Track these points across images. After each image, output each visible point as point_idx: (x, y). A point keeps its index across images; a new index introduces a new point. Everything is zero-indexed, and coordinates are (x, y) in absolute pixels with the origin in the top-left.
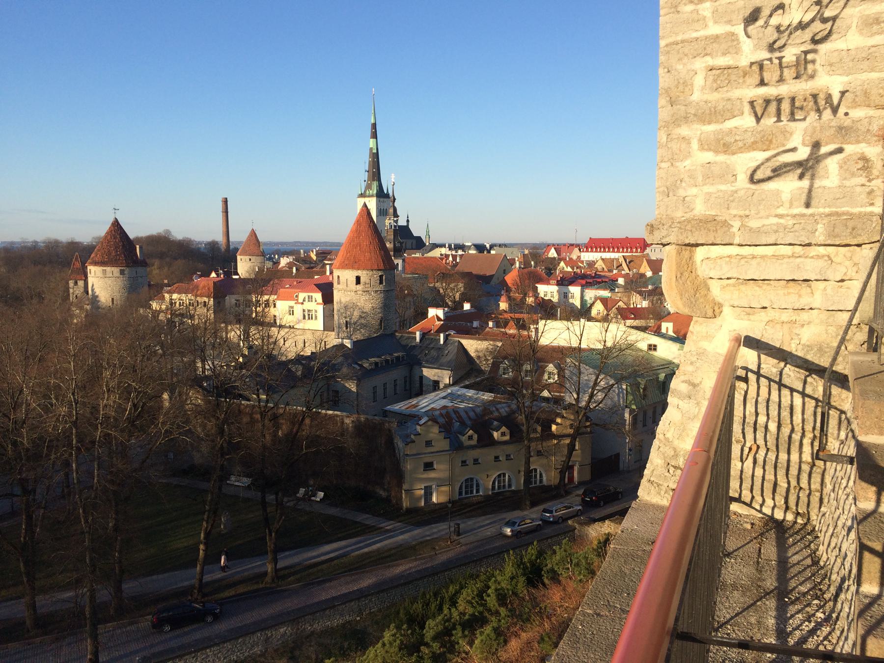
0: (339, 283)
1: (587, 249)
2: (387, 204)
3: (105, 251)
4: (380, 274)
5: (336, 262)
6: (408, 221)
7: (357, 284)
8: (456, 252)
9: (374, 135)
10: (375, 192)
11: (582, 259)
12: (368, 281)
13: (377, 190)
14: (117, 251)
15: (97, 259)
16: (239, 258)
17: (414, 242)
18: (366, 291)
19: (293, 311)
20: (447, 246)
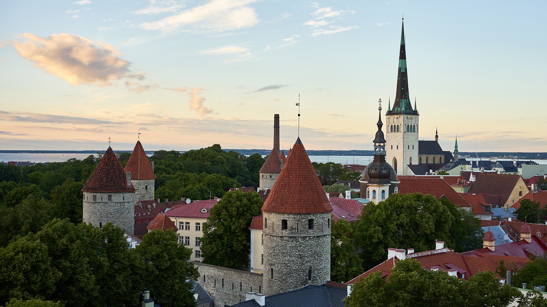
0: (266, 227)
4: (309, 218)
6: (437, 136)
8: (480, 170)
9: (403, 56)
10: (403, 109)
13: (405, 107)
14: (107, 178)
17: (443, 157)
20: (471, 163)
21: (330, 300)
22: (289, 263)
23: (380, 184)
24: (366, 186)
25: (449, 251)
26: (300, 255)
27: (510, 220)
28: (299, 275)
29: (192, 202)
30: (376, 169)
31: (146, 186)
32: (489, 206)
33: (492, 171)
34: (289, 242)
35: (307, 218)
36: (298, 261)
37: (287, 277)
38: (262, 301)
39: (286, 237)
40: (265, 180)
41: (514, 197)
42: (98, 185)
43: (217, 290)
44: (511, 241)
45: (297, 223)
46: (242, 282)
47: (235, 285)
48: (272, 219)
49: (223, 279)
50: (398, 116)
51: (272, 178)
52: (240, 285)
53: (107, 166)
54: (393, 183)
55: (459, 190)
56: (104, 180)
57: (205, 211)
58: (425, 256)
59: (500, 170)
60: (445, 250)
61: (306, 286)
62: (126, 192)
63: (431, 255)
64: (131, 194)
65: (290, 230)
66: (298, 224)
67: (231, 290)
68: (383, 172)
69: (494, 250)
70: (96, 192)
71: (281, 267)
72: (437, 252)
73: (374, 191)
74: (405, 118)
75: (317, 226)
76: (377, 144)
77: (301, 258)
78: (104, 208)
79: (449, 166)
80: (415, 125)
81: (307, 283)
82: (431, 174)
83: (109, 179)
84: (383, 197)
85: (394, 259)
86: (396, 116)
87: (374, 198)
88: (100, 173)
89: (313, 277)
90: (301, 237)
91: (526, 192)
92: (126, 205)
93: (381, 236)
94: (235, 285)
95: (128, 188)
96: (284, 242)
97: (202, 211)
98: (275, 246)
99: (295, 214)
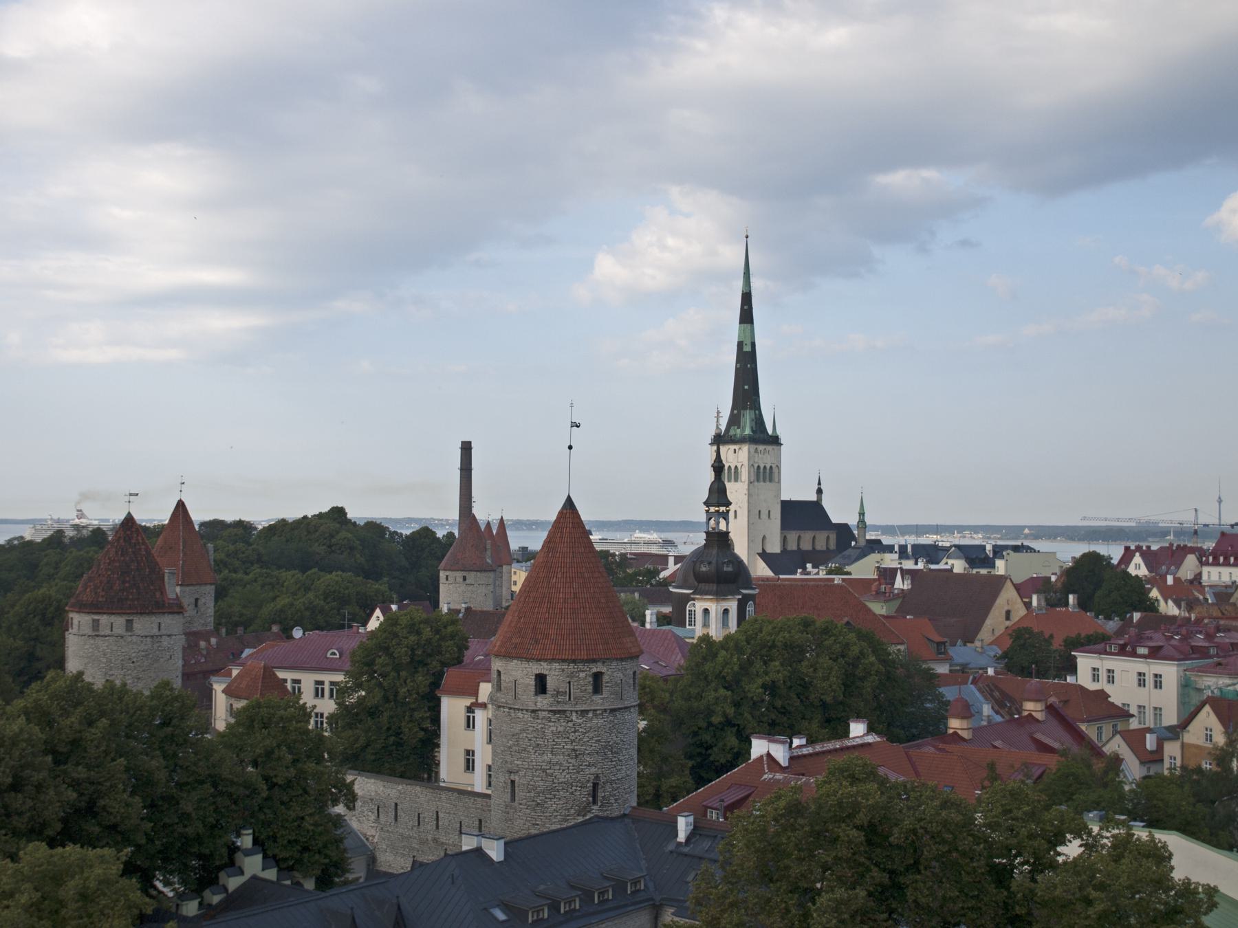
0: (498, 687)
1: (1216, 558)
2: (765, 456)
3: (101, 582)
4: (595, 670)
5: (496, 640)
6: (820, 491)
7: (536, 694)
8: (916, 563)
9: (747, 316)
10: (748, 431)
11: (1205, 577)
12: (564, 687)
13: (752, 428)
14: (124, 582)
15: (85, 599)
16: (442, 575)
17: (833, 537)
18: (559, 712)
19: (474, 717)
20: (896, 549)
21: (638, 846)
22: (550, 769)
23: (720, 595)
24: (687, 599)
25: (879, 739)
26: (574, 750)
27: (991, 672)
28: (572, 793)
29: (304, 634)
30: (710, 563)
31: (197, 600)
32: (944, 643)
33: (941, 566)
34: (550, 721)
35: (589, 671)
36: (570, 763)
37: (546, 798)
38: (495, 851)
39: (544, 711)
40: (451, 587)
41: (994, 624)
42: (103, 596)
43: (382, 829)
44: (998, 719)
45: (568, 680)
46: (439, 810)
47: (424, 818)
48: (514, 673)
49: (396, 804)
50: (736, 447)
51: (467, 582)
52: (435, 816)
53: (122, 555)
54: (749, 595)
55: (879, 608)
56: (116, 587)
57: (334, 654)
58: (830, 752)
59: (959, 566)
60: (871, 739)
61: (588, 817)
62: (164, 613)
63: (842, 749)
64: (176, 617)
65: (552, 696)
66: (569, 683)
67: (415, 828)
68: (725, 569)
69: (971, 737)
70: (99, 613)
71: (533, 776)
72: (855, 743)
73: (706, 611)
74: (752, 451)
75: (611, 687)
76: (712, 509)
77: (576, 756)
78: (115, 648)
79: (849, 556)
80: (774, 466)
81: (589, 811)
82: (809, 573)
83: (127, 585)
84: (725, 623)
85: (765, 758)
86: (732, 447)
87: (706, 624)
88: (107, 570)
89: (603, 797)
90: (576, 712)
91: (1020, 612)
92: (165, 642)
93: (731, 711)
94: (424, 818)
95: (169, 603)
96: (539, 721)
97: (329, 655)
98: (517, 731)
99: (564, 661)
